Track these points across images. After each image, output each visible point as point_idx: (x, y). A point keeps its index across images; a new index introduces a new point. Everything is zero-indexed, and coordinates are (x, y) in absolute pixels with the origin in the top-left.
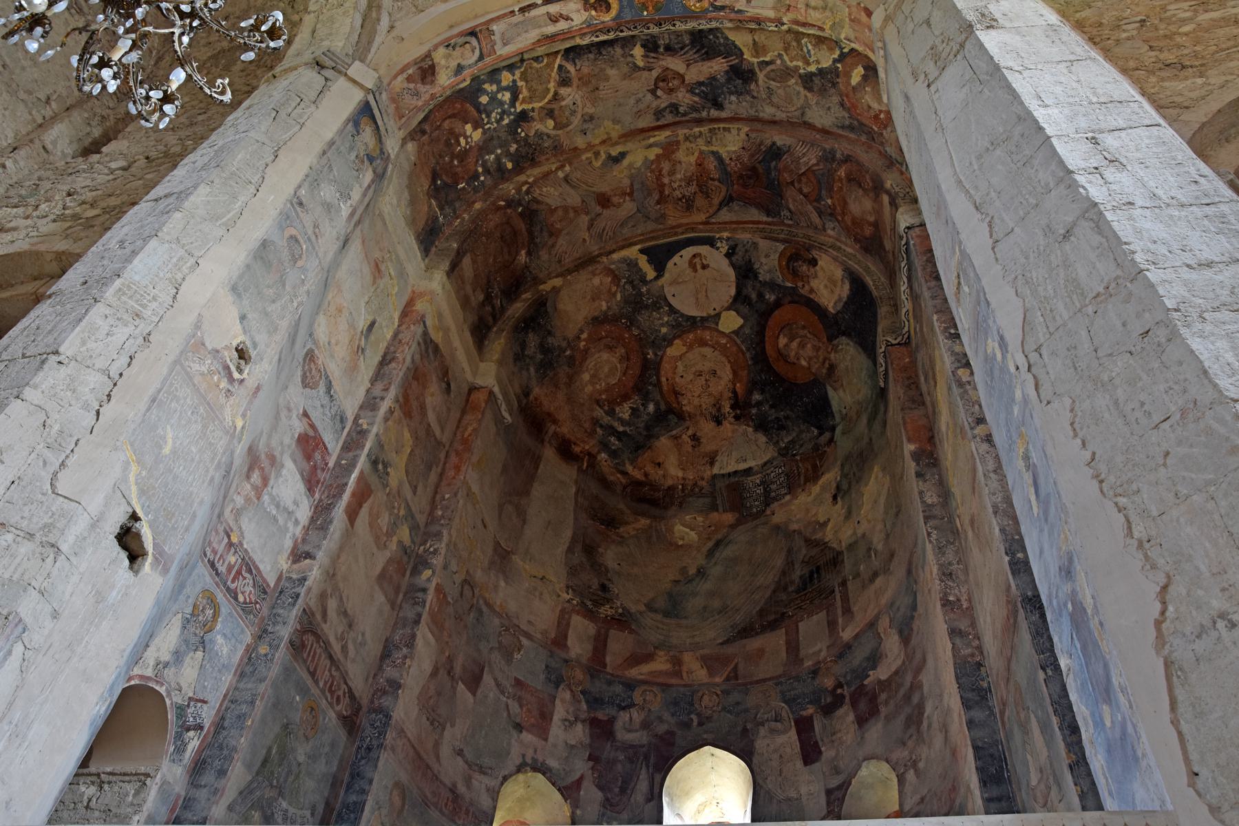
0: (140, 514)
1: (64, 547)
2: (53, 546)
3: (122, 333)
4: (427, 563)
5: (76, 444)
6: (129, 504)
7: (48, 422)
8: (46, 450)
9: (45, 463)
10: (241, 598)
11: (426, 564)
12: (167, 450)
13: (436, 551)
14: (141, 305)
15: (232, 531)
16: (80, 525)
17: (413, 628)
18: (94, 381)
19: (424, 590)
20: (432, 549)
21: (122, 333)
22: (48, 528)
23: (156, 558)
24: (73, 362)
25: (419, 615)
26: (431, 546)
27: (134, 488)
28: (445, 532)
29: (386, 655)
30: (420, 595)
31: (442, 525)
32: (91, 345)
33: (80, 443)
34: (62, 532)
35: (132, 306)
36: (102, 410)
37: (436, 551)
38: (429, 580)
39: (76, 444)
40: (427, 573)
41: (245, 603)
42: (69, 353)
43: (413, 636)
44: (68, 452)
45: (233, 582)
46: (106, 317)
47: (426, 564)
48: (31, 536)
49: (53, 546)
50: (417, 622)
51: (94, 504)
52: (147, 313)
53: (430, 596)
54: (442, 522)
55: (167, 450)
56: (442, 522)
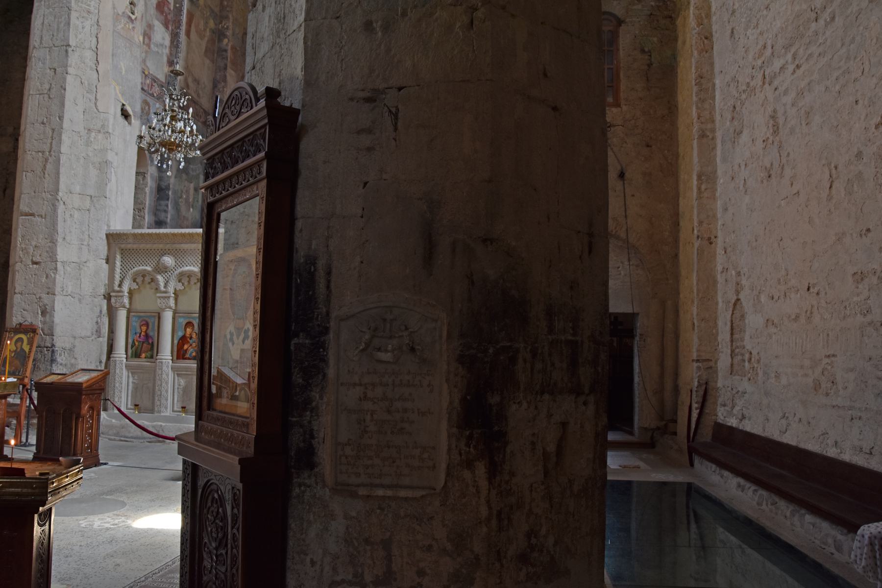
0: (124, 103)
1: (110, 131)
2: (107, 132)
3: (88, 24)
4: (225, 35)
5: (96, 88)
6: (120, 102)
7: (83, 81)
8: (88, 94)
9: (90, 100)
10: (155, 95)
11: (225, 36)
12: (124, 72)
13: (228, 27)
14: (87, 5)
15: (145, 70)
16: (111, 121)
17: (224, 72)
18: (89, 55)
19: (226, 51)
20: (225, 26)
21: (88, 24)
22: (103, 126)
23: (134, 116)
24: (77, 48)
25: (226, 65)
26: (225, 25)
27: (120, 95)
28: (230, 16)
29: (215, 86)
30: (224, 53)
31: (228, 11)
32: (80, 36)
33: (98, 87)
34: (108, 126)
35: (85, 7)
36: (98, 69)
37: (228, 27)
38: (227, 45)
39: (96, 88)
40: (226, 41)
41: (157, 96)
42: (74, 45)
43: (225, 76)
44: (95, 92)
45: (151, 90)
46: (78, 18)
47: (225, 36)
48: (99, 131)
49: (107, 132)
50: (225, 68)
51: (112, 111)
52: (92, 9)
53: (229, 54)
54: (228, 9)
55: (124, 72)
56: (228, 9)
